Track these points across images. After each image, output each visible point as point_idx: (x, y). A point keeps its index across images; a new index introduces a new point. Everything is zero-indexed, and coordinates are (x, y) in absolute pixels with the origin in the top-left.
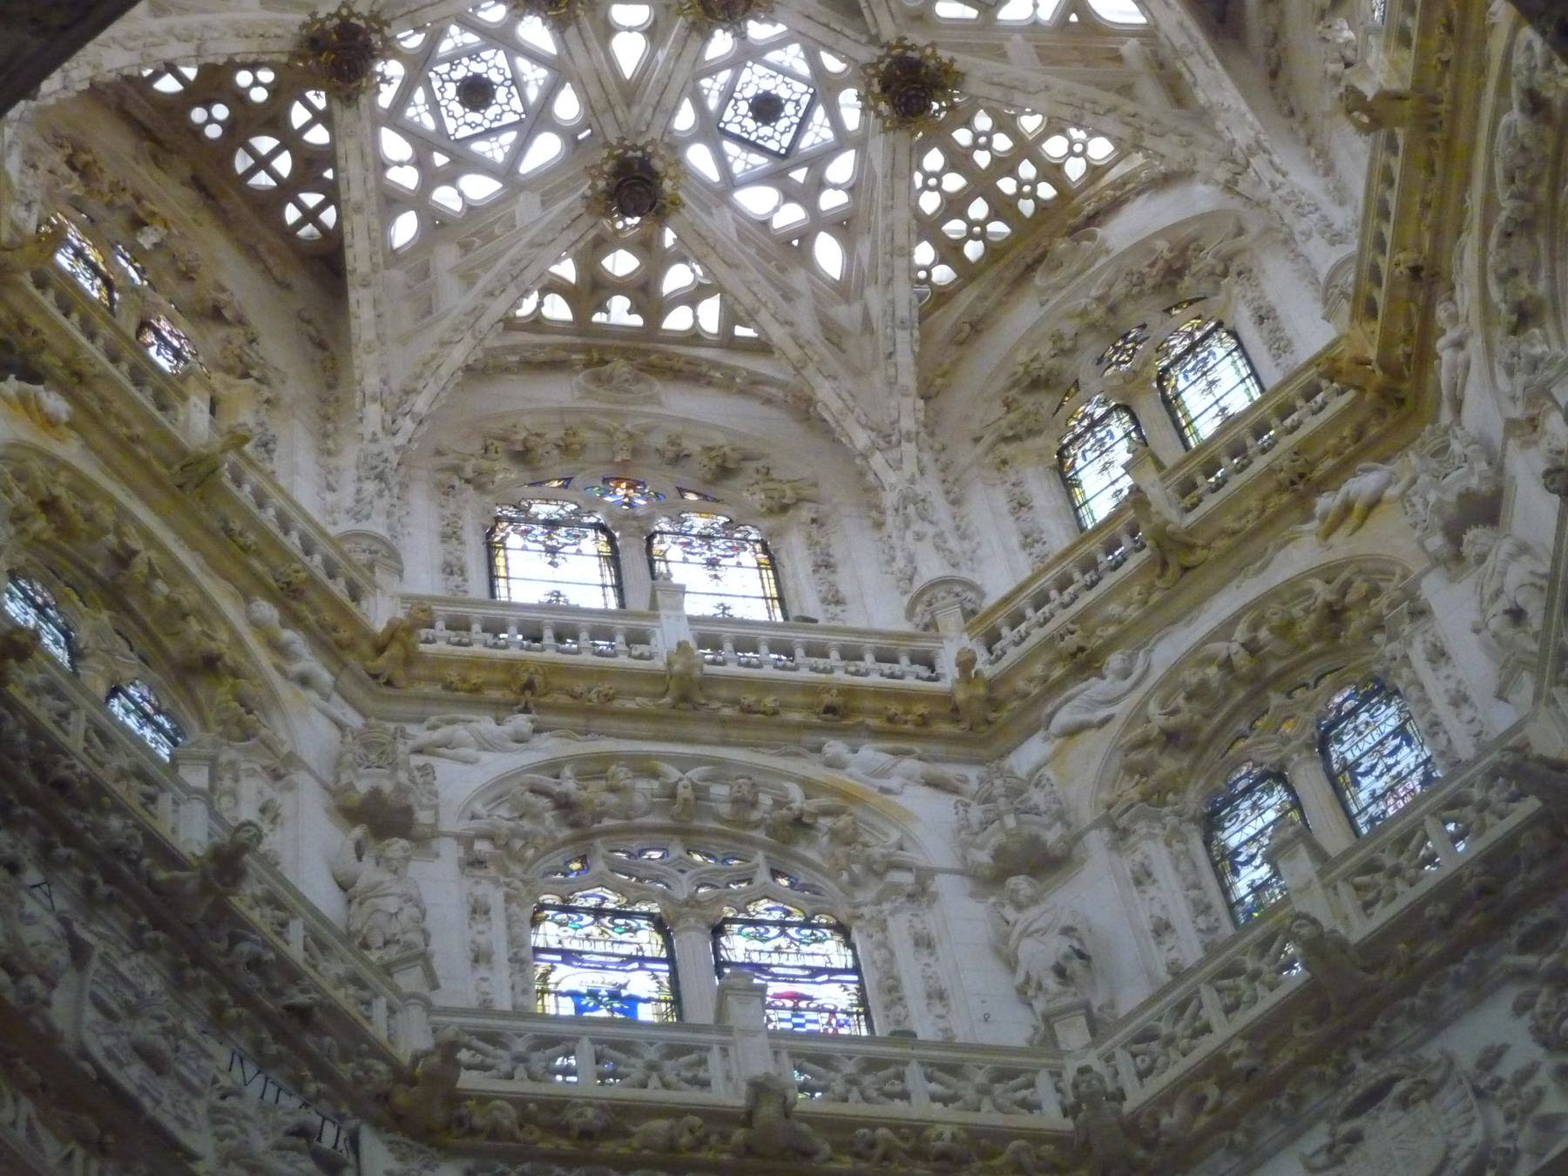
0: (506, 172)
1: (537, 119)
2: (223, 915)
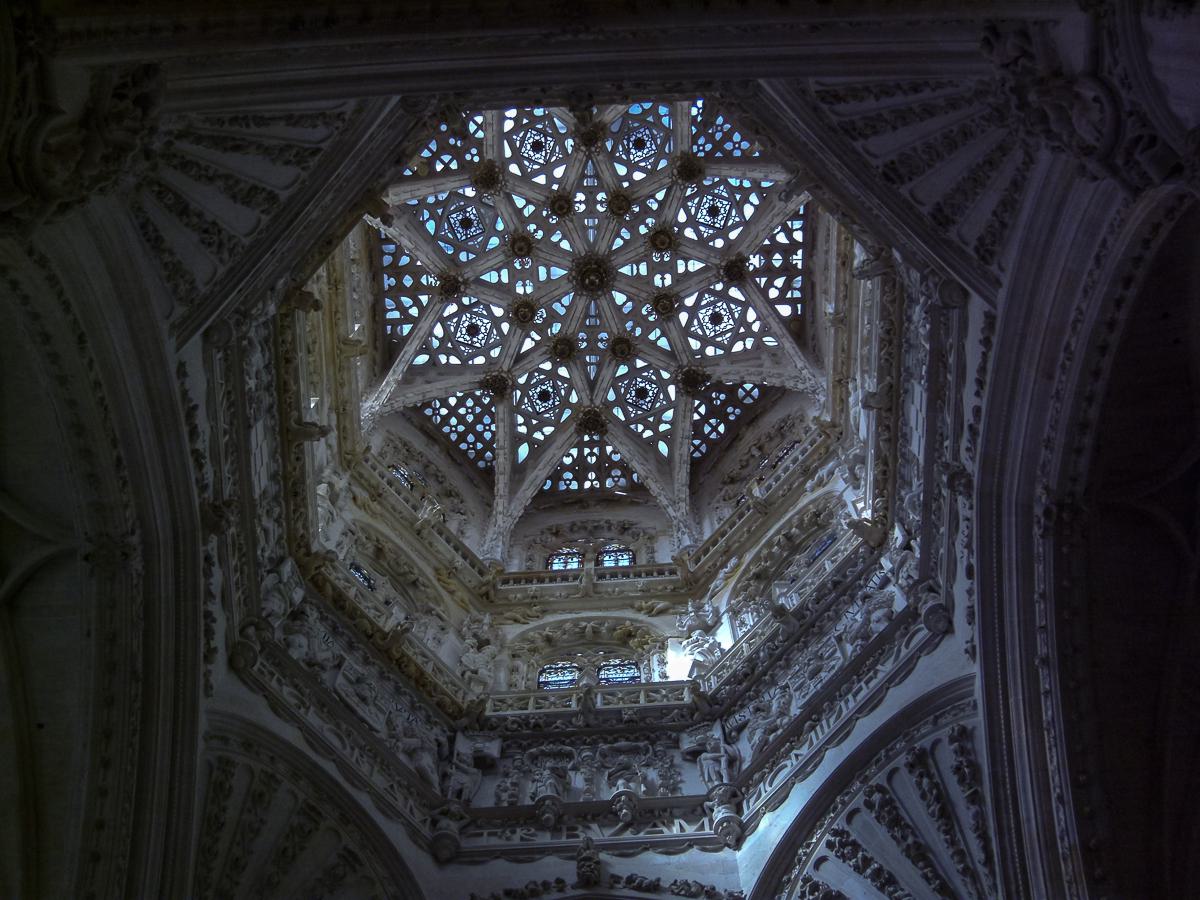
0: (745, 306)
1: (723, 295)
2: (799, 613)
